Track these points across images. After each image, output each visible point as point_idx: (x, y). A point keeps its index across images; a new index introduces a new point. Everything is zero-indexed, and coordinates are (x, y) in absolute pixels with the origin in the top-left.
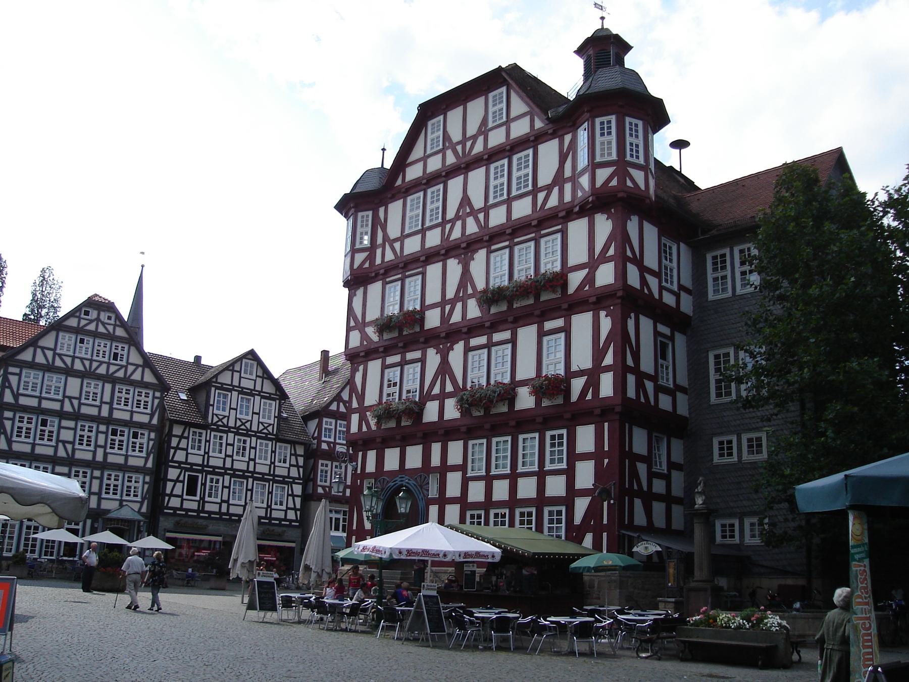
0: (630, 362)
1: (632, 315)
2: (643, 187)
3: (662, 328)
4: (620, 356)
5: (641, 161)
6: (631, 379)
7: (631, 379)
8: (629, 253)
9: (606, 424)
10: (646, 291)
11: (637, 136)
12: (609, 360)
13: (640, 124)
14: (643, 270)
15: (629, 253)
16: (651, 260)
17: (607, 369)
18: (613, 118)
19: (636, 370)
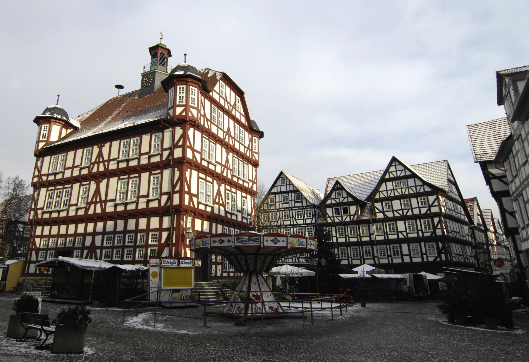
0: (186, 189)
1: (189, 170)
2: (196, 116)
3: (202, 175)
6: (187, 197)
8: (188, 144)
12: (178, 188)
14: (194, 151)
15: (188, 144)
16: (197, 147)
17: (177, 192)
19: (189, 193)
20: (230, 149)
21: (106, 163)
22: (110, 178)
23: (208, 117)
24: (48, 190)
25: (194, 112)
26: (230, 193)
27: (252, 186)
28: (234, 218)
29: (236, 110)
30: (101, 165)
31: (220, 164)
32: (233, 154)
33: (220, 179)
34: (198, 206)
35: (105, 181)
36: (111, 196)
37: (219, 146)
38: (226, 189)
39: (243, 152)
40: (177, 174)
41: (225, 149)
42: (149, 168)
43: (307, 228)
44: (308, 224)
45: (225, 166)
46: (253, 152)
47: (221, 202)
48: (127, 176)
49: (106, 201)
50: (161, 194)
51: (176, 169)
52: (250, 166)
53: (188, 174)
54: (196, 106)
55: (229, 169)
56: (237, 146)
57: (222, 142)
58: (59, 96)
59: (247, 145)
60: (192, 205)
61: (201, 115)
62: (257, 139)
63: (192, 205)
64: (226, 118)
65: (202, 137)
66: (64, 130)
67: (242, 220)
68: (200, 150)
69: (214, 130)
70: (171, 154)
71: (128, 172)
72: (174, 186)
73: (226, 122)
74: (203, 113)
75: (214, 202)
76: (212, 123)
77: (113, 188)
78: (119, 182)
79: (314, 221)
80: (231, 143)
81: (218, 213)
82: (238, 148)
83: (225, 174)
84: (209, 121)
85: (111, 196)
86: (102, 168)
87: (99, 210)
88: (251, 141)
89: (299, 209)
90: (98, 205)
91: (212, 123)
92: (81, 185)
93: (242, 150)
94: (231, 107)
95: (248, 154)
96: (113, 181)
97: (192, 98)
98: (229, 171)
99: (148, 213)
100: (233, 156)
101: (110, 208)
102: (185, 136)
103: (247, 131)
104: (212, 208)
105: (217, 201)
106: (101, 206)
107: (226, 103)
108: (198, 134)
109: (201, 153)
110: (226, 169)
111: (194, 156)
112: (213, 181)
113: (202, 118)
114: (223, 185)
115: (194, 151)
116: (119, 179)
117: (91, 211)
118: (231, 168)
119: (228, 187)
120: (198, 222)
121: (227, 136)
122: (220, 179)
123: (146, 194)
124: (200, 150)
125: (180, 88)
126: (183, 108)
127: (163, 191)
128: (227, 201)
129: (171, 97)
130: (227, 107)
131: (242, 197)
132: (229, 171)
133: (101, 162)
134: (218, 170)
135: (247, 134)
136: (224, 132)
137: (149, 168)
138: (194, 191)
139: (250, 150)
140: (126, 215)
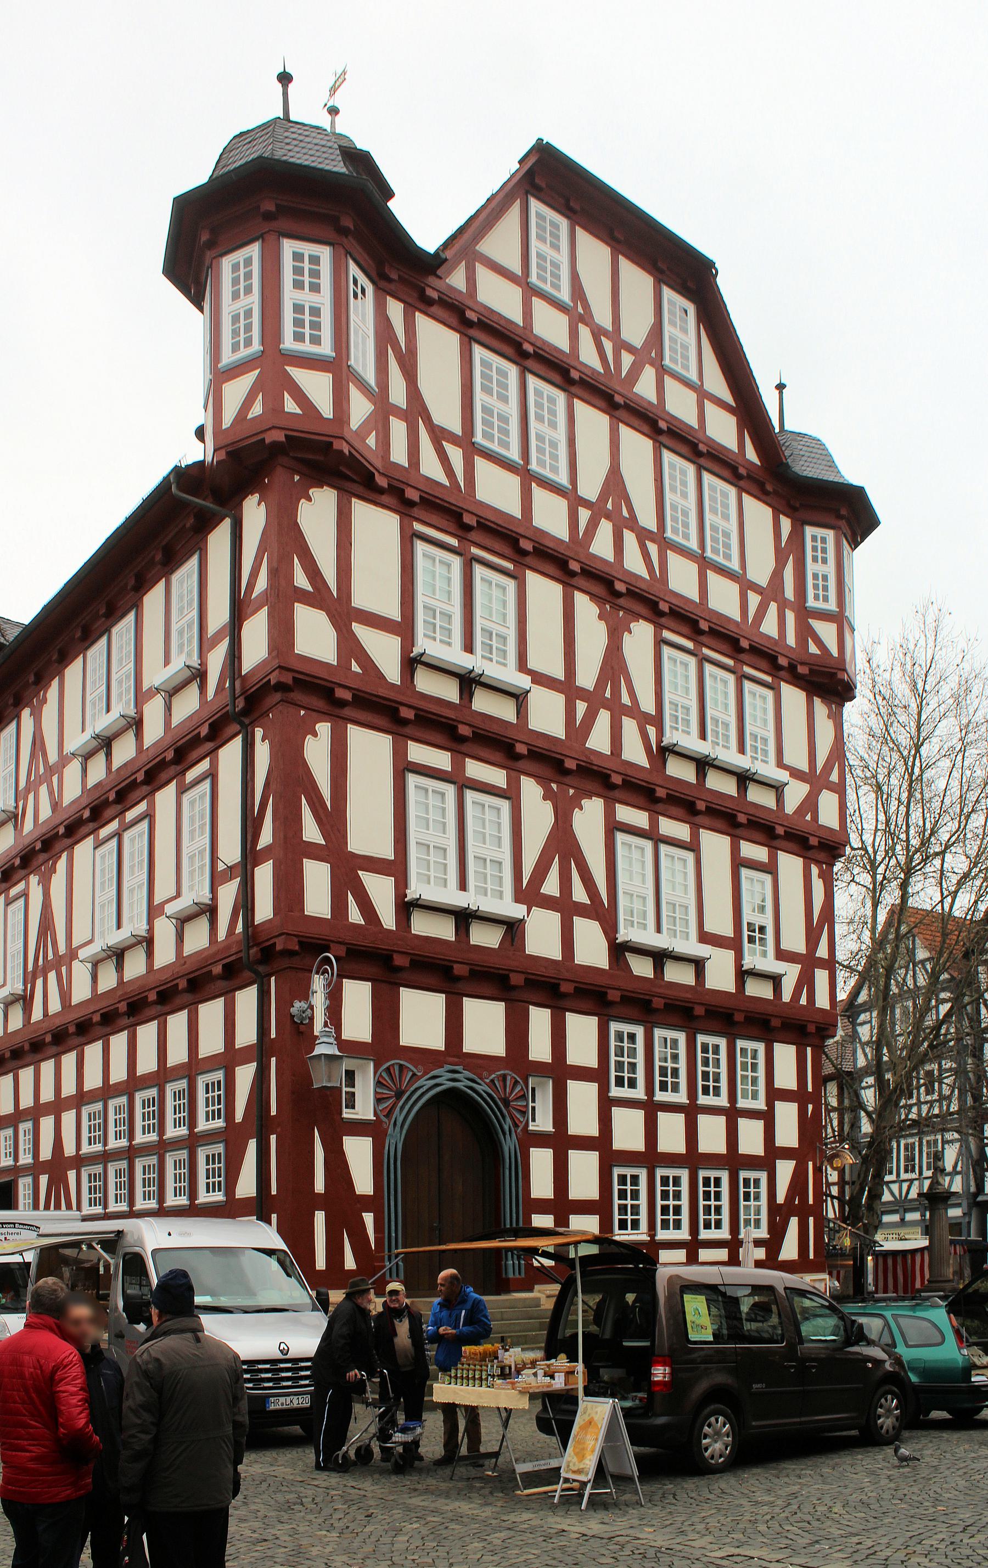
0: (311, 832)
8: (301, 580)
10: (355, 667)
11: (315, 288)
14: (343, 613)
15: (301, 580)
31: (567, 686)
32: (659, 627)
33: (568, 770)
37: (544, 592)
39: (736, 615)
40: (262, 752)
41: (593, 597)
47: (580, 894)
55: (634, 711)
56: (682, 579)
60: (355, 916)
63: (355, 916)
75: (529, 895)
81: (555, 953)
82: (694, 595)
83: (599, 740)
93: (724, 600)
95: (769, 627)
100: (660, 642)
102: (287, 540)
104: (513, 929)
105: (551, 886)
108: (376, 527)
109: (404, 628)
110: (604, 717)
111: (349, 646)
115: (343, 613)
118: (648, 706)
122: (568, 770)
124: (393, 612)
126: (249, 379)
134: (547, 716)
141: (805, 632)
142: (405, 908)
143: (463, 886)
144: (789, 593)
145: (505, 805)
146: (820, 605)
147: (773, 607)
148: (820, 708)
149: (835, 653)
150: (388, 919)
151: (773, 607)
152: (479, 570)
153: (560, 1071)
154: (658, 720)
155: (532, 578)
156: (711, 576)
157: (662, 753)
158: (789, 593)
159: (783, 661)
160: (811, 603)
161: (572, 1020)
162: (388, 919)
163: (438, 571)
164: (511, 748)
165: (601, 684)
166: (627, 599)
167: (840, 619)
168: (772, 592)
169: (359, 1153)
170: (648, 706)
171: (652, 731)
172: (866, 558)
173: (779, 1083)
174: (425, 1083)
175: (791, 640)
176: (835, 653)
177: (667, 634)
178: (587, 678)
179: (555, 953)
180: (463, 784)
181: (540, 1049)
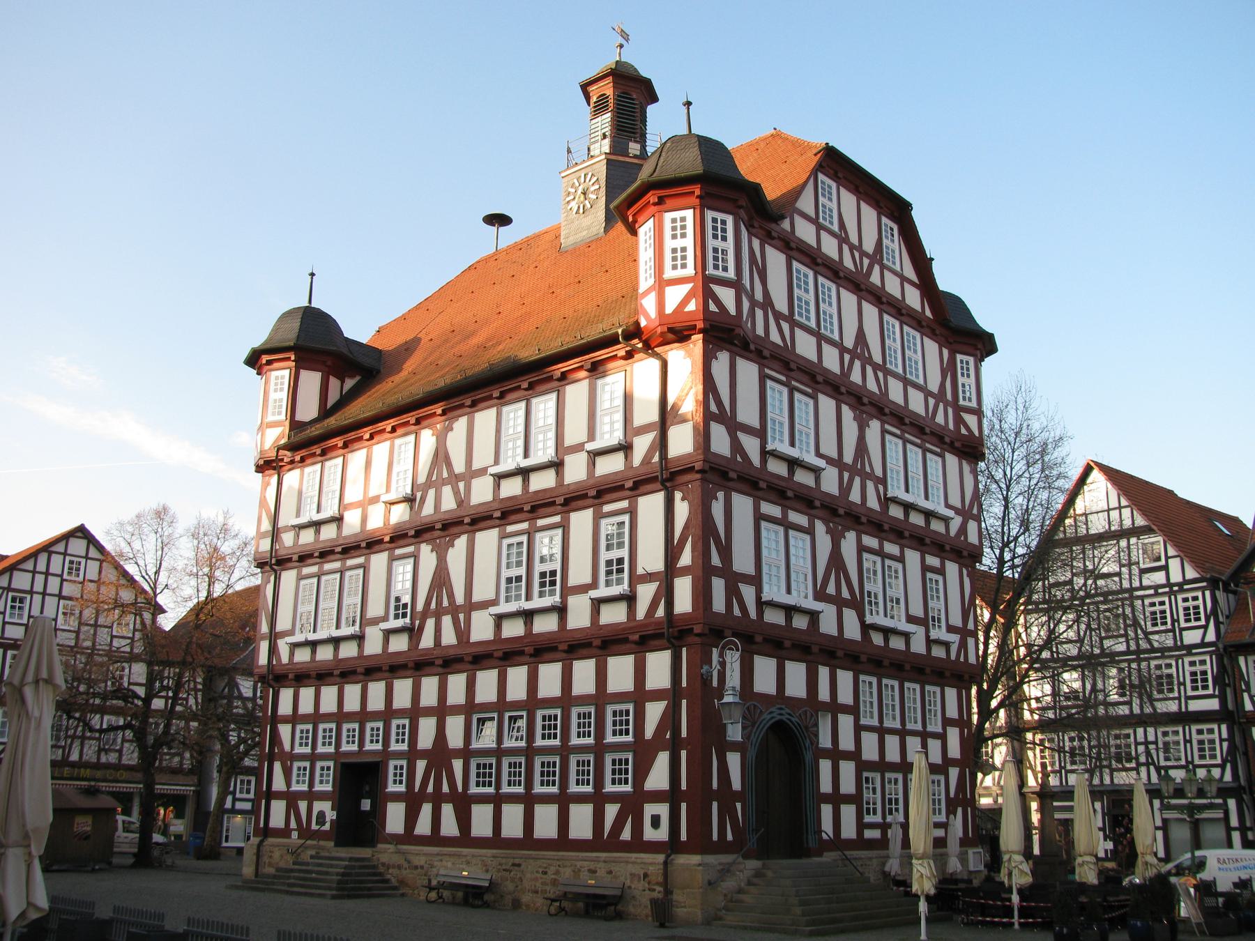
0: (716, 560)
1: (721, 495)
2: (733, 311)
4: (703, 554)
5: (731, 274)
6: (718, 585)
7: (718, 585)
9: (684, 650)
12: (686, 559)
13: (730, 220)
14: (734, 427)
16: (748, 413)
17: (685, 571)
18: (689, 214)
20: (870, 406)
21: (461, 485)
22: (475, 531)
23: (781, 305)
24: (300, 578)
25: (727, 296)
26: (878, 560)
27: (963, 530)
28: (897, 643)
29: (883, 267)
30: (447, 491)
31: (838, 463)
32: (883, 422)
33: (840, 515)
34: (760, 612)
35: (461, 542)
36: (483, 591)
37: (827, 404)
38: (861, 549)
40: (682, 510)
41: (852, 407)
42: (597, 494)
43: (1187, 660)
44: (1189, 649)
45: (857, 468)
46: (958, 409)
47: (845, 594)
48: (525, 525)
49: (472, 606)
50: (635, 580)
51: (678, 495)
52: (952, 460)
53: (717, 509)
54: (731, 274)
55: (871, 476)
56: (895, 392)
57: (838, 388)
58: (312, 275)
59: (934, 386)
60: (737, 612)
61: (754, 304)
62: (971, 360)
63: (737, 612)
64: (849, 299)
65: (763, 378)
66: (334, 383)
67: (929, 649)
68: (756, 423)
69: (805, 347)
70: (662, 443)
71: (533, 508)
72: (672, 553)
73: (847, 313)
74: (759, 296)
75: (820, 595)
76: (794, 324)
77: (484, 560)
78: (506, 542)
79: (1211, 636)
80: (872, 386)
81: (835, 632)
82: (901, 402)
84: (786, 319)
85: (483, 591)
86: (448, 503)
87: (449, 638)
88: (949, 370)
89: (1156, 594)
90: (447, 621)
91: (794, 324)
92: (392, 559)
93: (917, 403)
94: (866, 262)
95: (940, 419)
96: (487, 539)
97: (715, 250)
98: (870, 485)
99: (602, 643)
101: (481, 629)
103: (933, 336)
104: (814, 616)
105: (831, 589)
106: (456, 622)
107: (846, 248)
109: (761, 433)
110: (857, 480)
111: (736, 446)
112: (812, 524)
113: (759, 313)
114: (851, 536)
116: (503, 536)
117: (427, 641)
118: (879, 472)
119: (870, 541)
120: (765, 669)
121: (857, 364)
122: (840, 515)
123: (588, 580)
124: (756, 423)
125: (674, 221)
127: (640, 571)
128: (867, 587)
129: (646, 254)
130: (848, 263)
131: (925, 568)
132: (870, 485)
133: (445, 482)
134: (830, 483)
135: (932, 346)
136: (843, 350)
137: (597, 494)
138: (743, 562)
139: (946, 404)
140: (535, 651)
141: (959, 421)
142: (761, 604)
143: (789, 591)
144: (949, 397)
145: (808, 538)
146: (967, 404)
147: (941, 406)
148: (966, 468)
149: (977, 433)
150: (753, 614)
151: (941, 406)
152: (797, 395)
153: (835, 708)
154: (883, 481)
155: (821, 397)
156: (910, 389)
157: (886, 501)
158: (949, 397)
159: (947, 440)
160: (961, 402)
161: (840, 673)
162: (753, 614)
163: (777, 395)
164: (808, 501)
165: (855, 460)
166: (870, 406)
167: (978, 412)
168: (940, 396)
169: (734, 760)
170: (879, 472)
171: (881, 488)
172: (989, 363)
173: (948, 715)
174: (766, 716)
175: (951, 426)
176: (977, 433)
177: (887, 427)
178: (848, 458)
179: (835, 632)
180: (788, 526)
181: (824, 694)
